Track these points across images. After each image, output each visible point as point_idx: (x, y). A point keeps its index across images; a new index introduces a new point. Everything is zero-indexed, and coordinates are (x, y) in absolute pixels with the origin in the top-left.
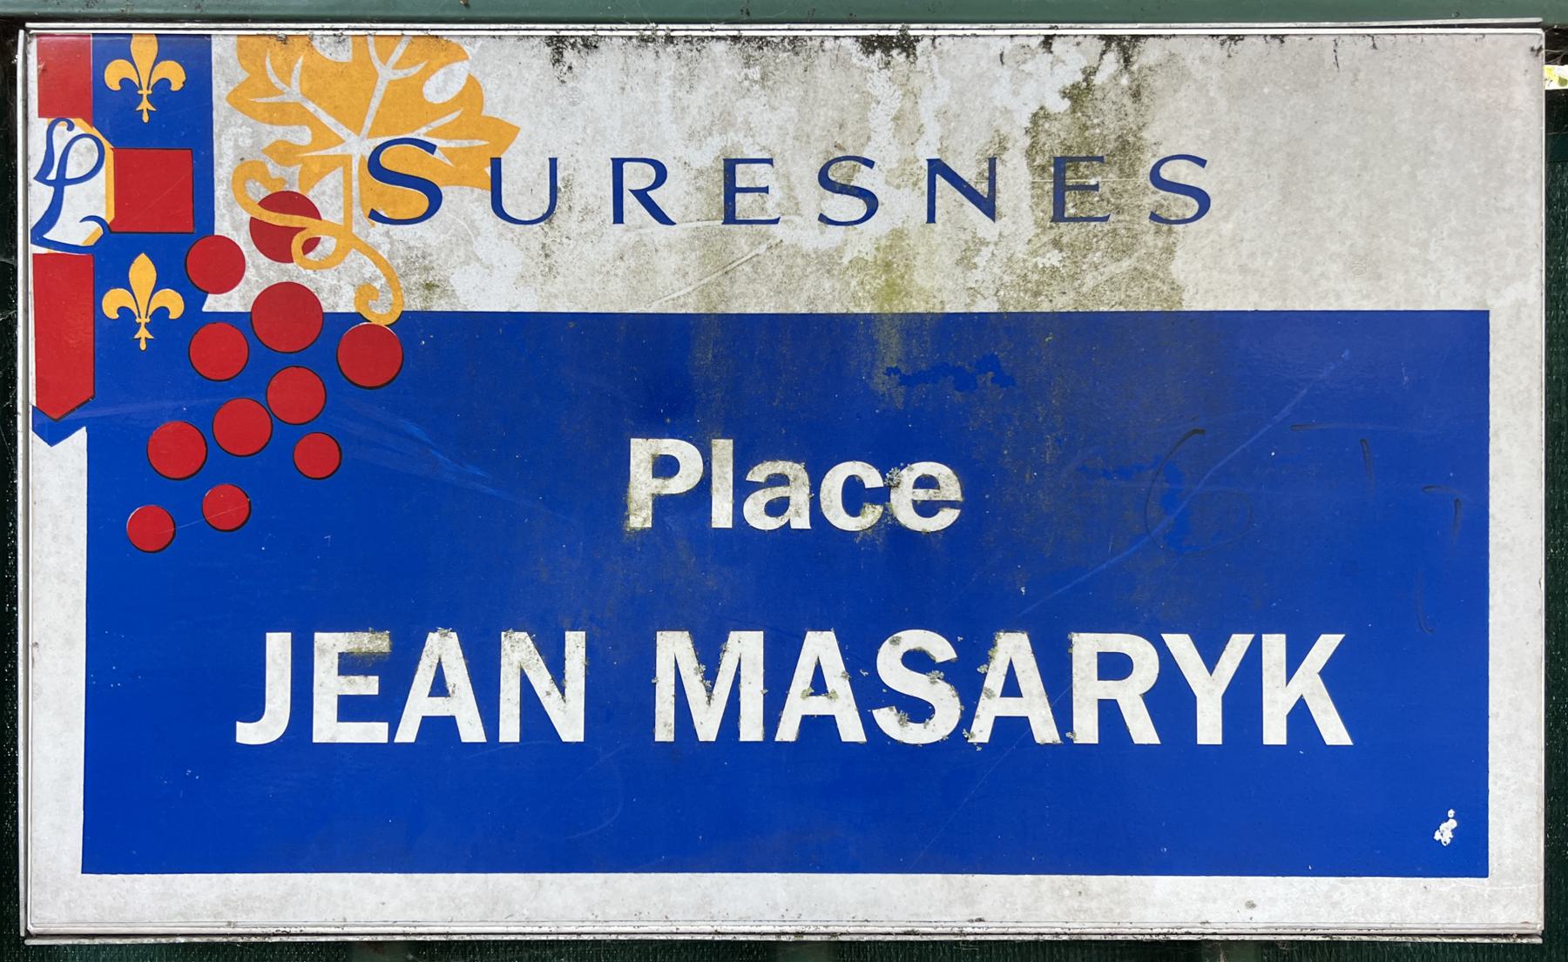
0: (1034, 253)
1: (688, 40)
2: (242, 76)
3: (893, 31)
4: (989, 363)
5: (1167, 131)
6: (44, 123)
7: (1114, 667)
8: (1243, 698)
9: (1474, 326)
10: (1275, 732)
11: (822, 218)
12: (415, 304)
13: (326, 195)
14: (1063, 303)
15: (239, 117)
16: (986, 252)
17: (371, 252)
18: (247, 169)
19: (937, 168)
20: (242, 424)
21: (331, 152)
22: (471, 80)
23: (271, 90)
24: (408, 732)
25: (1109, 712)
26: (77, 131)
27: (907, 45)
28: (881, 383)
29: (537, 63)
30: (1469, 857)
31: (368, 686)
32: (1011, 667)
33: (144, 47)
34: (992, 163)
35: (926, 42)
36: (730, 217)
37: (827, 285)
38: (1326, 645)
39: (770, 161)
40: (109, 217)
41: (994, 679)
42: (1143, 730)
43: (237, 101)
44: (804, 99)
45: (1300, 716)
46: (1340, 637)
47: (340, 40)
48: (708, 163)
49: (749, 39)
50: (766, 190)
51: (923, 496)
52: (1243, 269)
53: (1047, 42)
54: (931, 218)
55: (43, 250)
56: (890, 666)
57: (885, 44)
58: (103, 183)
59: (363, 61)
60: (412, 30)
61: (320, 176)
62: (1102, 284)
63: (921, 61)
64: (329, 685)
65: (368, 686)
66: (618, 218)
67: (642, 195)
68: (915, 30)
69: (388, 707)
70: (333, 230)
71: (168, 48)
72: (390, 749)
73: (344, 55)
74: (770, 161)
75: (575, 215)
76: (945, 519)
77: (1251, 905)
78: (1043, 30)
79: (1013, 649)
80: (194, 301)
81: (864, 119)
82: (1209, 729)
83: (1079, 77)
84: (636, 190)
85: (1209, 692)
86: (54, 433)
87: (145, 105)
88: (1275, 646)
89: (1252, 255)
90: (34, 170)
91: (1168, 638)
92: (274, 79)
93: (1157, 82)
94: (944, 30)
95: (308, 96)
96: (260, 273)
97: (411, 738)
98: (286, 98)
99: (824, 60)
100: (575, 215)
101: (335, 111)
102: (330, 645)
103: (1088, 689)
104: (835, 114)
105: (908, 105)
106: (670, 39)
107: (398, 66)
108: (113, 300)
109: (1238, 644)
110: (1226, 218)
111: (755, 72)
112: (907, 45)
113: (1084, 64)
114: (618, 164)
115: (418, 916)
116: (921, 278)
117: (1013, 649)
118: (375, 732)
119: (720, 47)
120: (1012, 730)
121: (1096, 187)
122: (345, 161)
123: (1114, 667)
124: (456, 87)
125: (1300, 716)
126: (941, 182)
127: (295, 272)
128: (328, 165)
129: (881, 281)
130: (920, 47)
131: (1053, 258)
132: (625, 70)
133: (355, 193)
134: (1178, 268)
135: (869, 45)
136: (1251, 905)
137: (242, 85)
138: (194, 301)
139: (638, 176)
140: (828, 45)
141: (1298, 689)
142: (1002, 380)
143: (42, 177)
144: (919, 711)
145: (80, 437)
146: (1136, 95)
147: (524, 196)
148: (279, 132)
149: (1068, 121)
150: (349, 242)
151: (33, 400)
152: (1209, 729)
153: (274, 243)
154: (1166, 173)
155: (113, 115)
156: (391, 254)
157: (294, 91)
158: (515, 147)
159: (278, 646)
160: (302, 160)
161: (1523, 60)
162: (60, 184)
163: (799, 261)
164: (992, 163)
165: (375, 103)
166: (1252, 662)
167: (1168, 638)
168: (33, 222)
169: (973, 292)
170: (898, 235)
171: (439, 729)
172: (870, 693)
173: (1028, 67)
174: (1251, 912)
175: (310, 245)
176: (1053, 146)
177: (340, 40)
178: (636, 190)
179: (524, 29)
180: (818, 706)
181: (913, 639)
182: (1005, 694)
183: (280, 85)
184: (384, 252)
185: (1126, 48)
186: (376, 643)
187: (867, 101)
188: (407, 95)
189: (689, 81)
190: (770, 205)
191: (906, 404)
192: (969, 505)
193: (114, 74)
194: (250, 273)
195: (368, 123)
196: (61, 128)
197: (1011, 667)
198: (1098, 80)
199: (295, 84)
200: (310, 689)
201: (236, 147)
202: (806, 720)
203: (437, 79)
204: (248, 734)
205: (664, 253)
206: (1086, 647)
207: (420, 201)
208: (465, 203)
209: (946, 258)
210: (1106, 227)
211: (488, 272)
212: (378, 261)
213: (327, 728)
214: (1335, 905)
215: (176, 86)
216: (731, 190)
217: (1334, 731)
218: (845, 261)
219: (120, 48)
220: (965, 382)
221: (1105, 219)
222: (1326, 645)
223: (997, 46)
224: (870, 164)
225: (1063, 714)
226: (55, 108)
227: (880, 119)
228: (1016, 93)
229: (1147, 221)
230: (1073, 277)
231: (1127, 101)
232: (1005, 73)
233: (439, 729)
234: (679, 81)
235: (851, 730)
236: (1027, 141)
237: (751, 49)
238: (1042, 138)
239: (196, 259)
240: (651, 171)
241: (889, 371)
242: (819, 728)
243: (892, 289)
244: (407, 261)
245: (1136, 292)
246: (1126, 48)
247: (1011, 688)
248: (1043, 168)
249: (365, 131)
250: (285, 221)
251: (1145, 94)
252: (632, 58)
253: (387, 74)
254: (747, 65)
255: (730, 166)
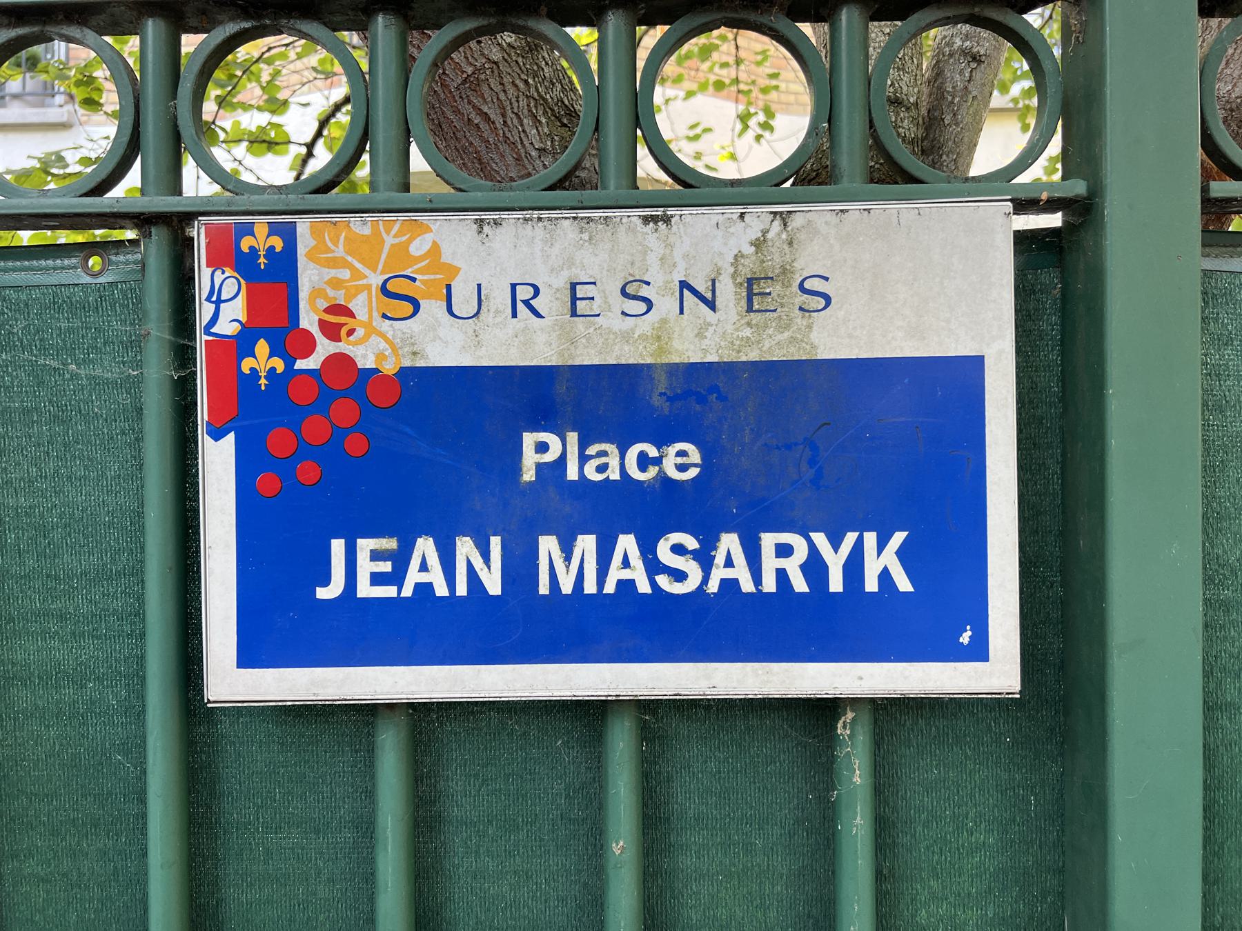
0: (737, 330)
1: (550, 219)
2: (313, 243)
3: (659, 211)
4: (714, 389)
5: (807, 262)
6: (210, 270)
7: (784, 551)
8: (854, 566)
9: (977, 363)
10: (871, 585)
11: (623, 313)
12: (407, 363)
13: (358, 305)
14: (753, 355)
15: (312, 265)
16: (711, 329)
17: (382, 335)
18: (316, 293)
19: (684, 285)
20: (315, 428)
21: (361, 282)
22: (434, 243)
23: (329, 250)
24: (407, 591)
25: (782, 575)
26: (227, 274)
27: (667, 220)
28: (656, 401)
29: (469, 233)
30: (979, 651)
31: (386, 567)
32: (729, 551)
33: (261, 225)
34: (714, 281)
35: (677, 218)
36: (574, 313)
37: (626, 348)
38: (899, 538)
39: (594, 283)
40: (244, 319)
41: (720, 559)
42: (800, 585)
43: (310, 256)
44: (612, 250)
45: (885, 576)
46: (906, 533)
47: (364, 223)
48: (562, 285)
49: (582, 218)
50: (593, 298)
51: (680, 461)
52: (850, 336)
53: (742, 215)
54: (681, 312)
55: (210, 338)
56: (664, 552)
57: (655, 219)
58: (241, 301)
59: (376, 233)
60: (402, 217)
61: (355, 296)
62: (774, 346)
63: (674, 227)
64: (365, 568)
65: (386, 567)
66: (514, 315)
67: (526, 303)
68: (670, 211)
69: (396, 578)
70: (363, 324)
71: (274, 229)
72: (398, 600)
73: (367, 231)
74: (594, 283)
75: (491, 314)
76: (693, 473)
77: (861, 678)
78: (740, 209)
79: (730, 542)
80: (289, 364)
81: (644, 260)
82: (836, 584)
83: (760, 234)
84: (523, 300)
85: (836, 562)
86: (217, 435)
87: (262, 260)
88: (870, 538)
89: (855, 328)
90: (204, 296)
91: (813, 535)
92: (330, 244)
93: (802, 236)
94: (686, 211)
95: (348, 253)
96: (325, 348)
97: (409, 594)
98: (336, 255)
99: (622, 229)
100: (491, 314)
101: (362, 261)
102: (365, 545)
103: (770, 563)
104: (629, 258)
105: (668, 252)
106: (540, 219)
107: (395, 236)
108: (247, 365)
109: (850, 538)
110: (840, 309)
111: (586, 236)
112: (667, 220)
113: (762, 227)
114: (513, 286)
115: (414, 688)
116: (676, 344)
117: (730, 542)
118: (390, 592)
119: (567, 222)
120: (730, 585)
121: (769, 294)
122: (368, 287)
123: (784, 551)
124: (426, 247)
125: (885, 576)
126: (686, 292)
127: (342, 347)
128: (359, 290)
129: (655, 346)
130: (673, 220)
131: (747, 332)
132: (517, 236)
133: (374, 304)
134: (814, 336)
135: (646, 220)
136: (861, 678)
137: (313, 248)
138: (289, 364)
139: (524, 293)
140: (624, 220)
141: (884, 561)
142: (722, 398)
143: (208, 299)
144: (680, 576)
145: (231, 437)
146: (790, 244)
147: (464, 302)
148: (333, 273)
149: (754, 258)
150: (371, 330)
151: (206, 418)
152: (836, 584)
153: (332, 332)
154: (807, 285)
155: (245, 265)
156: (394, 337)
157: (340, 251)
158: (458, 278)
159: (338, 547)
160: (346, 287)
161: (1001, 219)
162: (218, 302)
163: (612, 336)
164: (714, 281)
165: (384, 256)
166: (859, 547)
167: (813, 535)
168: (204, 324)
169: (705, 351)
170: (664, 321)
171: (424, 589)
172: (654, 567)
173: (732, 230)
174: (860, 682)
175: (351, 332)
176: (746, 272)
177: (364, 223)
178: (523, 300)
179: (462, 215)
180: (626, 574)
181: (676, 538)
182: (725, 566)
183: (333, 247)
184: (390, 335)
185: (784, 218)
186: (390, 544)
187: (645, 250)
188: (401, 252)
189: (550, 242)
190: (595, 307)
191: (670, 411)
192: (705, 466)
193: (246, 244)
194: (319, 348)
195: (380, 267)
196: (218, 272)
197: (729, 551)
198: (770, 236)
199: (341, 246)
200: (356, 568)
201: (310, 280)
202: (620, 582)
203: (417, 242)
204: (322, 593)
205: (539, 333)
206: (769, 541)
207: (408, 308)
208: (432, 308)
209: (690, 333)
210: (775, 315)
211: (443, 344)
212: (387, 340)
213: (365, 590)
214: (906, 678)
215: (278, 249)
216: (574, 299)
217: (904, 584)
218: (636, 336)
219: (249, 230)
220: (702, 400)
221: (775, 311)
222: (899, 538)
223: (715, 219)
224: (648, 283)
225: (757, 577)
226: (215, 262)
227: (653, 259)
228: (725, 244)
229: (797, 311)
230: (758, 342)
231: (786, 247)
232: (719, 233)
233: (424, 589)
234: (545, 241)
235: (644, 587)
236: (732, 270)
237: (583, 224)
238: (740, 268)
239: (290, 341)
240: (531, 290)
241: (661, 394)
242: (626, 586)
243: (661, 351)
244: (402, 340)
245: (792, 349)
246: (784, 218)
247: (729, 563)
248: (741, 284)
249: (379, 271)
250: (337, 320)
251: (795, 242)
252: (520, 230)
253: (389, 240)
254: (581, 232)
255: (573, 286)
